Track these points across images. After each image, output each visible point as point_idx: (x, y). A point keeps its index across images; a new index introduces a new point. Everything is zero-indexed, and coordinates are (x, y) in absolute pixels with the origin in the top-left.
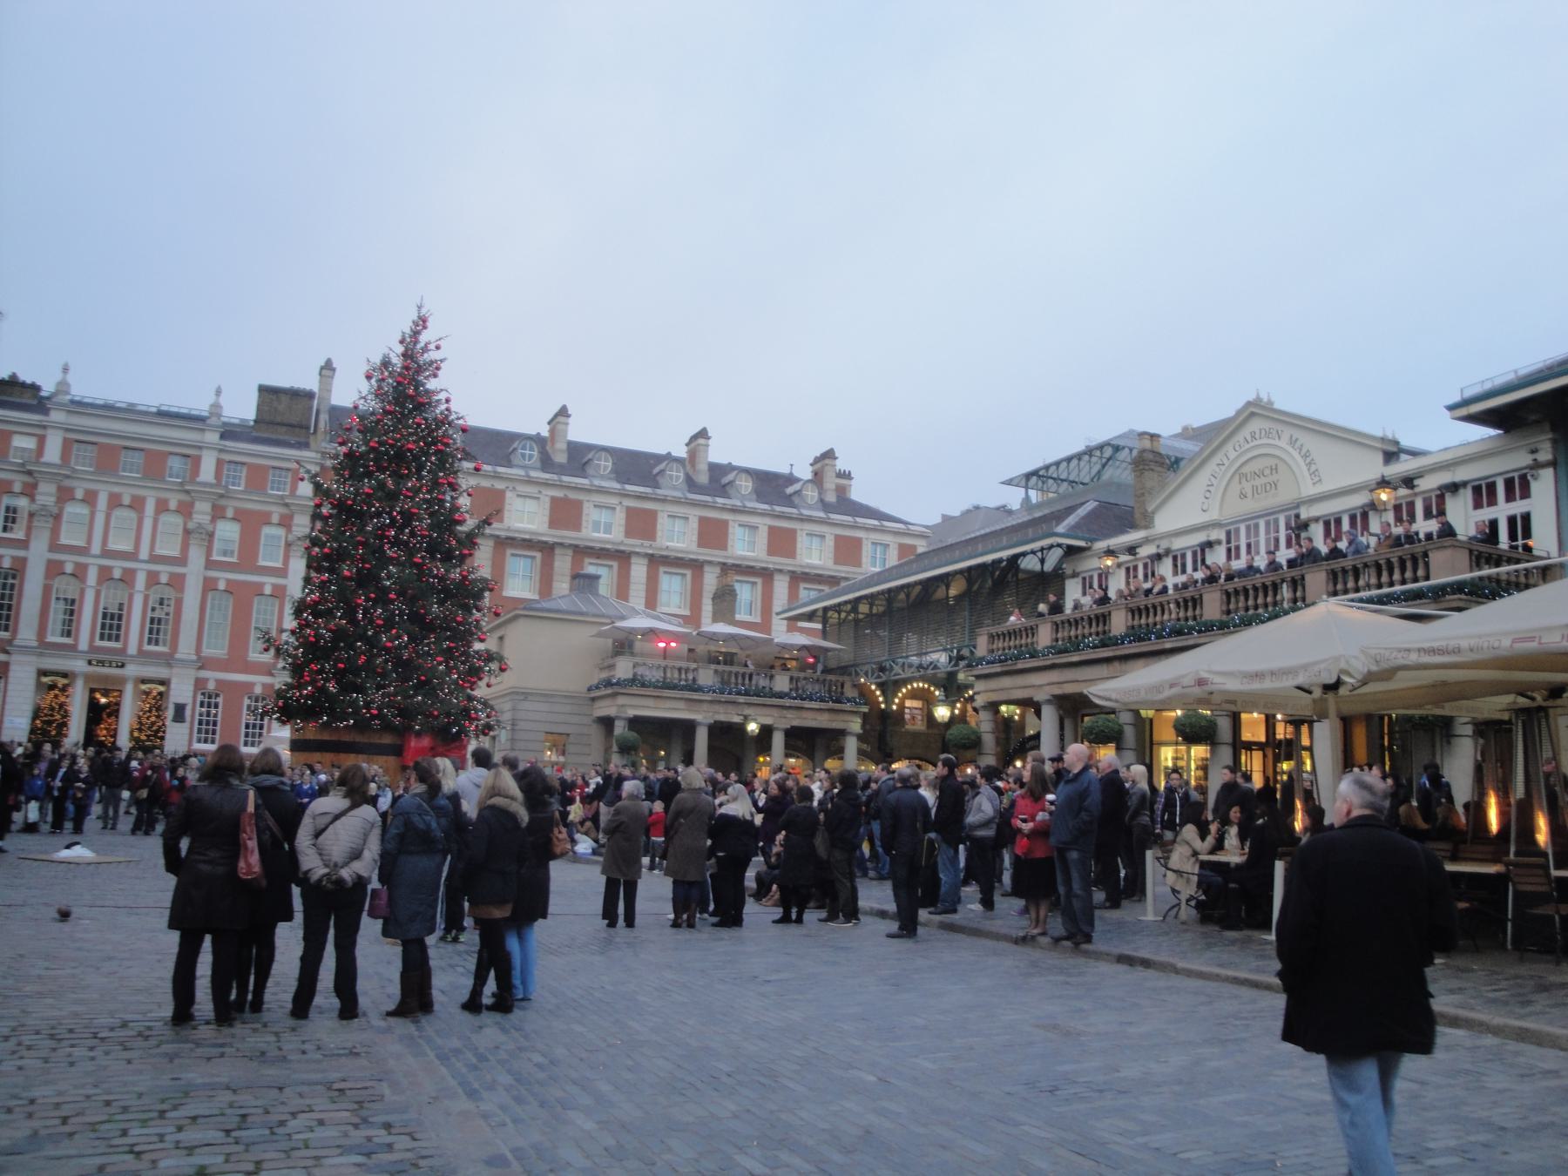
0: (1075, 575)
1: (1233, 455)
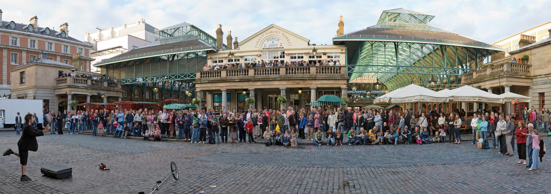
0: (211, 58)
1: (265, 36)
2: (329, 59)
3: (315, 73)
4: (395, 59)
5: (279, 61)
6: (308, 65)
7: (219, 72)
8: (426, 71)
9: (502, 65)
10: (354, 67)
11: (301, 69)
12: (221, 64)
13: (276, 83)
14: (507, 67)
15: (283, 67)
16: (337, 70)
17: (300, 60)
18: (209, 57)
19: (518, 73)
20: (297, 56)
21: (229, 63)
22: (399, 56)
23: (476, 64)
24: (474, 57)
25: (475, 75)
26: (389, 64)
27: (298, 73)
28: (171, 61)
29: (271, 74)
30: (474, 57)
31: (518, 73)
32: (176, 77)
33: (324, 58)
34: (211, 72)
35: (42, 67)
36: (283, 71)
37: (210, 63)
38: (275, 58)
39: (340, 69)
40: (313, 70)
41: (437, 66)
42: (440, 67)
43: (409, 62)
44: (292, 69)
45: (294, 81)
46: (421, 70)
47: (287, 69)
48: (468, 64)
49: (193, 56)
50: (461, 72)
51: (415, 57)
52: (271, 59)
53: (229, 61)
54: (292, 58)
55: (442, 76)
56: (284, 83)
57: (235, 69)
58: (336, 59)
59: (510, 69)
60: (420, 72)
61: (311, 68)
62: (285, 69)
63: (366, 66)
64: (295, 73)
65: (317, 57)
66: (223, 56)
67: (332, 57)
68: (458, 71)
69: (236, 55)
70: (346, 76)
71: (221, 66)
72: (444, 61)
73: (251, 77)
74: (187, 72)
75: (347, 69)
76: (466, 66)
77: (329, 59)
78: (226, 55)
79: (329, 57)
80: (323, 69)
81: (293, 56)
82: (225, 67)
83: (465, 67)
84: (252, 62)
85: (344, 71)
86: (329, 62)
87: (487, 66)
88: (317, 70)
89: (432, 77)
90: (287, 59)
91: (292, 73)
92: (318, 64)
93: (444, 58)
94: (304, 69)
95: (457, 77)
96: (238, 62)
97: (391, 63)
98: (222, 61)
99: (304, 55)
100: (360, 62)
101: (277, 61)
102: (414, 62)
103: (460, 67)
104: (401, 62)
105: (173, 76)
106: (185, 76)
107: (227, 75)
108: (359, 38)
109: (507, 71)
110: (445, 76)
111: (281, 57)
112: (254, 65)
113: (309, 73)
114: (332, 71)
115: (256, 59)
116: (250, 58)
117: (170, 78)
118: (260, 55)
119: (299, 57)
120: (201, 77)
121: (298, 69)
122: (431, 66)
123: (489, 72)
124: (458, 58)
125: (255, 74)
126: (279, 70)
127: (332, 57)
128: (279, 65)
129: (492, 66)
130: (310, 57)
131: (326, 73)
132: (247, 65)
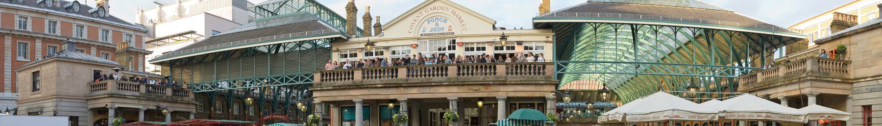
0: (338, 51)
2: (527, 52)
3: (504, 74)
4: (632, 51)
5: (447, 54)
6: (493, 61)
7: (350, 73)
8: (682, 70)
9: (804, 61)
10: (566, 64)
11: (481, 67)
12: (353, 59)
14: (812, 65)
15: (453, 65)
16: (539, 69)
17: (481, 53)
19: (829, 74)
20: (475, 46)
21: (367, 58)
22: (639, 47)
23: (763, 60)
24: (759, 48)
25: (760, 77)
26: (623, 59)
27: (477, 74)
28: (274, 55)
29: (433, 75)
30: (759, 48)
31: (829, 74)
32: (282, 81)
33: (519, 50)
34: (338, 73)
35: (67, 65)
36: (452, 71)
37: (336, 57)
38: (440, 49)
39: (544, 68)
40: (501, 69)
41: (700, 63)
42: (705, 64)
43: (655, 56)
44: (468, 68)
46: (674, 70)
47: (459, 68)
48: (749, 60)
49: (309, 46)
50: (737, 72)
51: (664, 49)
52: (434, 52)
53: (367, 54)
54: (467, 49)
55: (707, 78)
57: (376, 67)
58: (538, 52)
59: (816, 68)
60: (672, 73)
61: (498, 66)
62: (456, 68)
63: (586, 62)
64: (472, 74)
65: (508, 48)
66: (357, 46)
67: (531, 49)
68: (734, 71)
69: (377, 45)
70: (555, 79)
71: (353, 63)
72: (711, 55)
73: (402, 80)
74: (299, 73)
75: (555, 67)
76: (746, 62)
77: (527, 52)
78: (362, 46)
79: (526, 48)
80: (517, 67)
81: (470, 46)
82: (360, 65)
83: (744, 65)
84: (404, 56)
85: (551, 70)
86: (526, 55)
87: (779, 63)
88: (507, 68)
89: (692, 80)
90: (460, 52)
91: (468, 74)
92: (509, 60)
93: (710, 51)
94: (486, 67)
95: (731, 79)
96: (380, 57)
97: (626, 58)
98: (355, 55)
99: (486, 46)
100: (576, 56)
101: (444, 55)
102: (662, 56)
103: (737, 65)
104: (642, 56)
105: (277, 78)
106: (297, 79)
107: (364, 78)
109: (812, 71)
110: (712, 79)
111: (450, 48)
112: (407, 61)
113: (495, 73)
114: (532, 71)
115: (409, 52)
116: (400, 49)
117: (272, 81)
118: (417, 46)
119: (478, 49)
120: (323, 80)
121: (477, 67)
122: (691, 62)
123: (782, 71)
124: (733, 50)
125: (408, 76)
126: (447, 69)
127: (531, 49)
128: (447, 60)
129: (787, 63)
130: (496, 48)
131: (521, 74)
132: (396, 62)
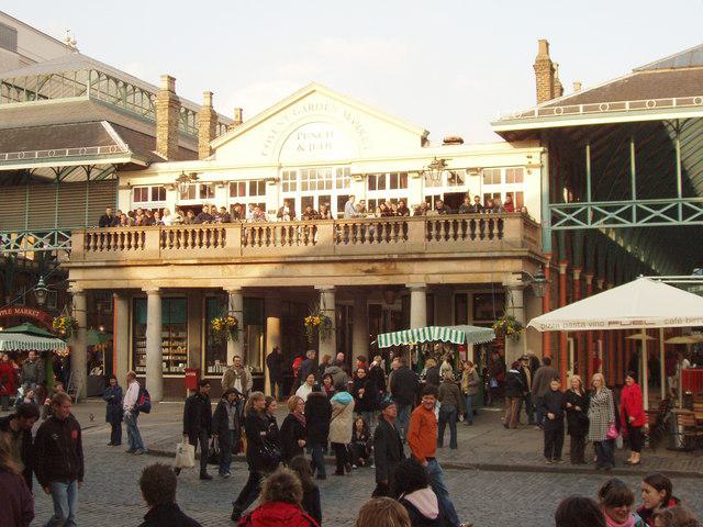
13: (306, 270)
18: (122, 182)
45: (360, 265)
56: (329, 270)
108: (558, 118)
114: (478, 231)
131: (260, 243)
